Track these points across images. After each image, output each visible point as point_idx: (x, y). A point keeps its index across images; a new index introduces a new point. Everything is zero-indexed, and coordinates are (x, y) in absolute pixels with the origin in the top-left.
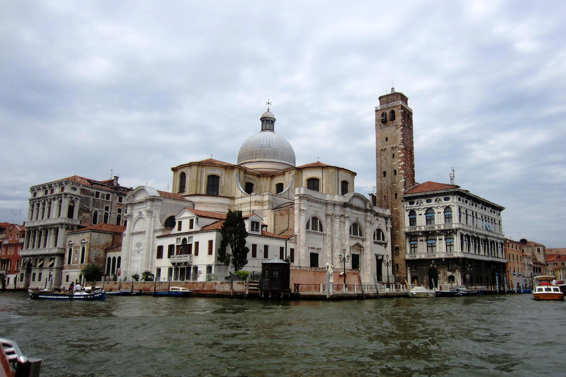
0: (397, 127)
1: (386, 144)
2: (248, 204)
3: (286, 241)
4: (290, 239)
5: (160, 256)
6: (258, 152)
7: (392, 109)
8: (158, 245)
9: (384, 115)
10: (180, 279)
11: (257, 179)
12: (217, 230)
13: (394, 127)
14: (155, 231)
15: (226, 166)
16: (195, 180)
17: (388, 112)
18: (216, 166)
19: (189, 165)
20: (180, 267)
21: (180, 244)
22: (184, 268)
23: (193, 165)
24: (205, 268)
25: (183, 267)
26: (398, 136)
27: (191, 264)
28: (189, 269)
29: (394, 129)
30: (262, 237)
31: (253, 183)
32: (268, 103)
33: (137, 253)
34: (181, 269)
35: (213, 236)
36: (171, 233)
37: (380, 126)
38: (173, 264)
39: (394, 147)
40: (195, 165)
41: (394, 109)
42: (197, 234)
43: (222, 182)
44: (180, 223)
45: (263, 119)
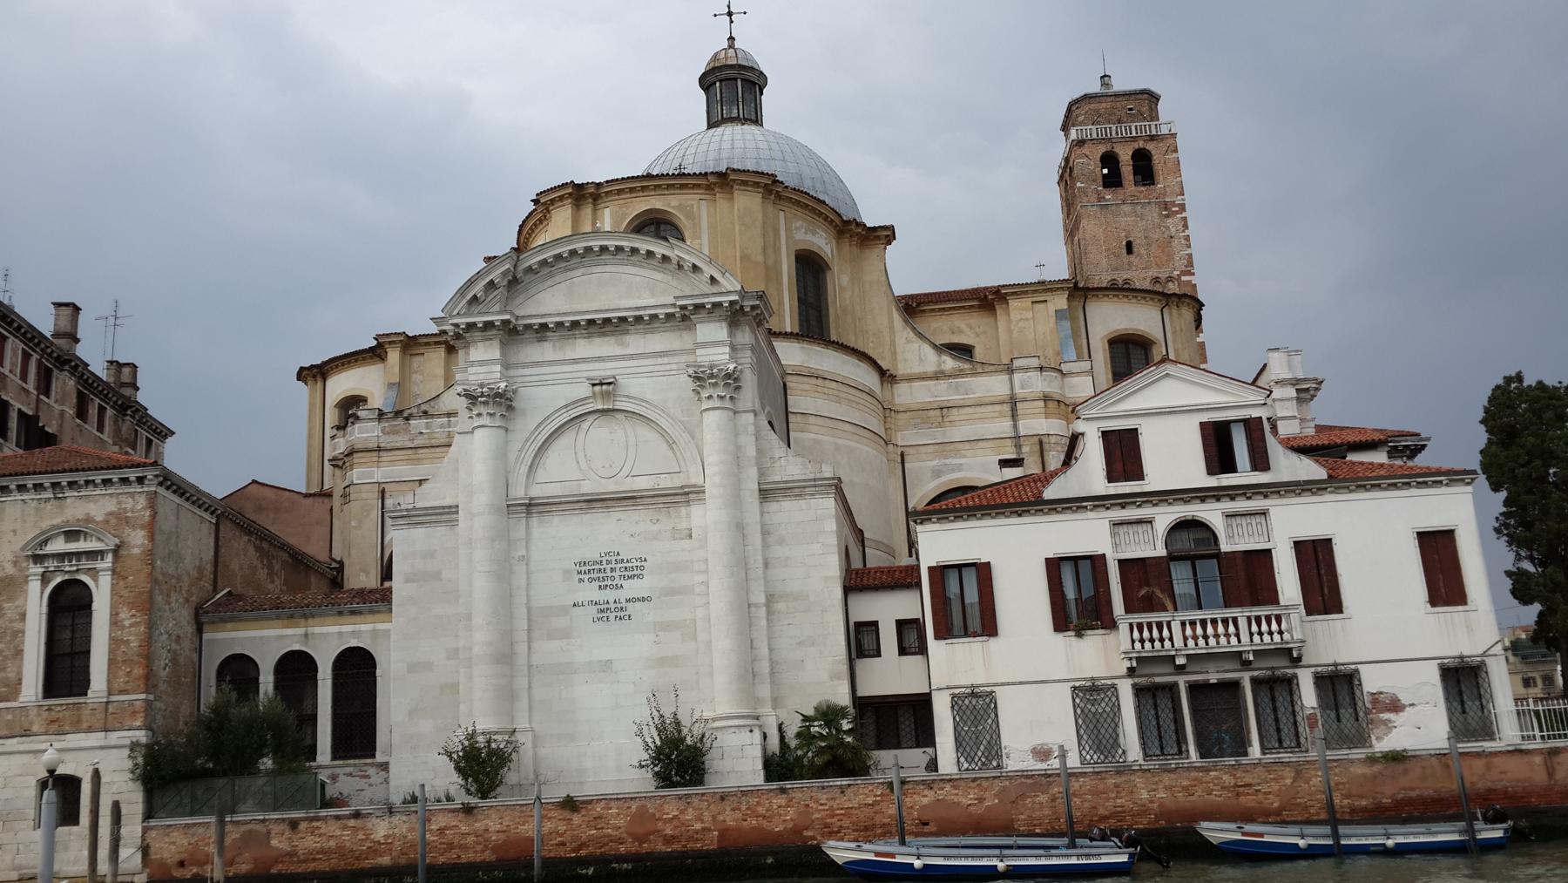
0: (1166, 209)
1: (1130, 264)
2: (998, 408)
7: (1141, 144)
9: (1109, 160)
13: (1155, 209)
15: (849, 222)
16: (760, 258)
17: (1125, 155)
18: (820, 214)
19: (712, 179)
22: (1235, 686)
23: (745, 183)
24: (1432, 674)
25: (1213, 678)
26: (1175, 242)
29: (1155, 215)
32: (730, 14)
34: (1194, 688)
37: (1100, 198)
39: (1163, 276)
40: (757, 184)
41: (1150, 146)
42: (1307, 498)
45: (712, 78)
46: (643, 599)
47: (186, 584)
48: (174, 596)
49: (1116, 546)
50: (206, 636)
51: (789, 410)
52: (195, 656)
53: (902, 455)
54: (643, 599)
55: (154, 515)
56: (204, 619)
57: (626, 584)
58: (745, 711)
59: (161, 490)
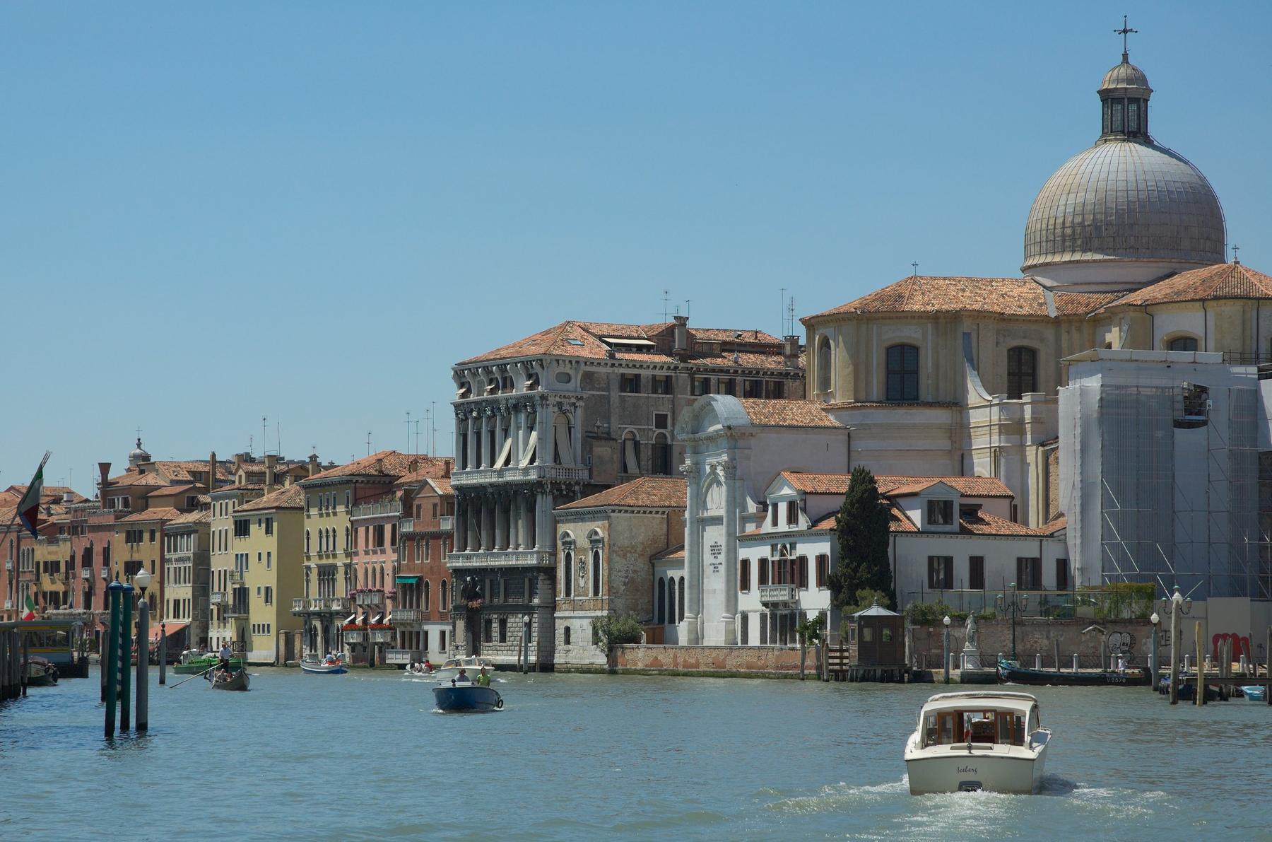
3: (1041, 541)
4: (1055, 534)
5: (745, 585)
6: (1068, 231)
8: (741, 559)
10: (781, 639)
11: (1049, 333)
12: (832, 533)
14: (745, 519)
18: (907, 317)
20: (779, 613)
21: (777, 558)
22: (786, 615)
27: (793, 606)
28: (793, 616)
30: (960, 536)
31: (1036, 347)
32: (1125, 31)
33: (714, 571)
34: (781, 616)
35: (825, 548)
36: (761, 533)
38: (765, 604)
40: (849, 320)
43: (927, 363)
44: (775, 506)
46: (721, 564)
47: (640, 548)
48: (628, 555)
49: (772, 556)
50: (656, 569)
51: (851, 449)
52: (651, 577)
53: (963, 455)
54: (721, 564)
55: (609, 526)
56: (653, 561)
57: (719, 556)
58: (728, 615)
59: (612, 514)
